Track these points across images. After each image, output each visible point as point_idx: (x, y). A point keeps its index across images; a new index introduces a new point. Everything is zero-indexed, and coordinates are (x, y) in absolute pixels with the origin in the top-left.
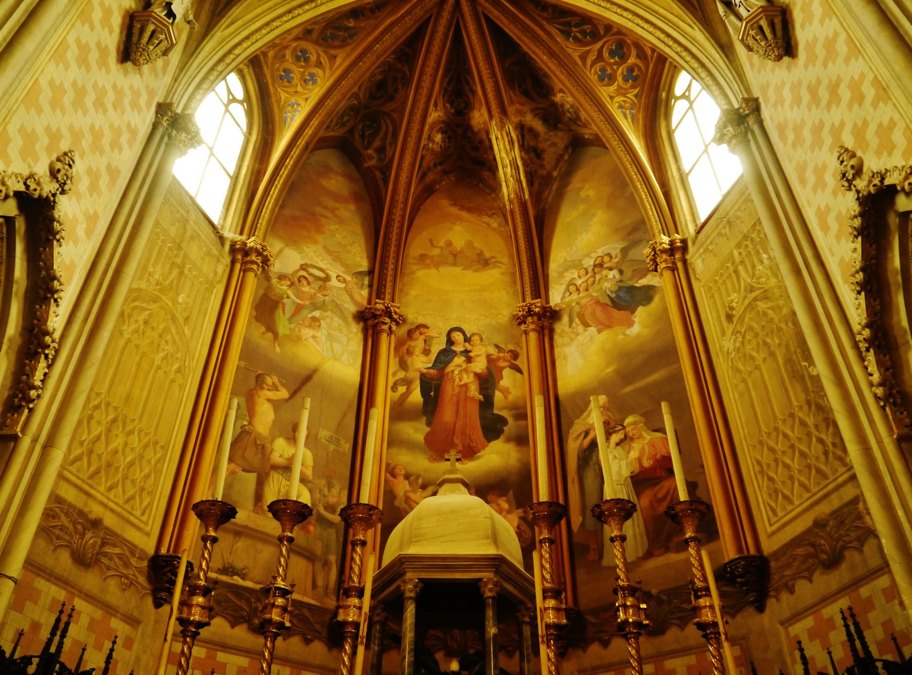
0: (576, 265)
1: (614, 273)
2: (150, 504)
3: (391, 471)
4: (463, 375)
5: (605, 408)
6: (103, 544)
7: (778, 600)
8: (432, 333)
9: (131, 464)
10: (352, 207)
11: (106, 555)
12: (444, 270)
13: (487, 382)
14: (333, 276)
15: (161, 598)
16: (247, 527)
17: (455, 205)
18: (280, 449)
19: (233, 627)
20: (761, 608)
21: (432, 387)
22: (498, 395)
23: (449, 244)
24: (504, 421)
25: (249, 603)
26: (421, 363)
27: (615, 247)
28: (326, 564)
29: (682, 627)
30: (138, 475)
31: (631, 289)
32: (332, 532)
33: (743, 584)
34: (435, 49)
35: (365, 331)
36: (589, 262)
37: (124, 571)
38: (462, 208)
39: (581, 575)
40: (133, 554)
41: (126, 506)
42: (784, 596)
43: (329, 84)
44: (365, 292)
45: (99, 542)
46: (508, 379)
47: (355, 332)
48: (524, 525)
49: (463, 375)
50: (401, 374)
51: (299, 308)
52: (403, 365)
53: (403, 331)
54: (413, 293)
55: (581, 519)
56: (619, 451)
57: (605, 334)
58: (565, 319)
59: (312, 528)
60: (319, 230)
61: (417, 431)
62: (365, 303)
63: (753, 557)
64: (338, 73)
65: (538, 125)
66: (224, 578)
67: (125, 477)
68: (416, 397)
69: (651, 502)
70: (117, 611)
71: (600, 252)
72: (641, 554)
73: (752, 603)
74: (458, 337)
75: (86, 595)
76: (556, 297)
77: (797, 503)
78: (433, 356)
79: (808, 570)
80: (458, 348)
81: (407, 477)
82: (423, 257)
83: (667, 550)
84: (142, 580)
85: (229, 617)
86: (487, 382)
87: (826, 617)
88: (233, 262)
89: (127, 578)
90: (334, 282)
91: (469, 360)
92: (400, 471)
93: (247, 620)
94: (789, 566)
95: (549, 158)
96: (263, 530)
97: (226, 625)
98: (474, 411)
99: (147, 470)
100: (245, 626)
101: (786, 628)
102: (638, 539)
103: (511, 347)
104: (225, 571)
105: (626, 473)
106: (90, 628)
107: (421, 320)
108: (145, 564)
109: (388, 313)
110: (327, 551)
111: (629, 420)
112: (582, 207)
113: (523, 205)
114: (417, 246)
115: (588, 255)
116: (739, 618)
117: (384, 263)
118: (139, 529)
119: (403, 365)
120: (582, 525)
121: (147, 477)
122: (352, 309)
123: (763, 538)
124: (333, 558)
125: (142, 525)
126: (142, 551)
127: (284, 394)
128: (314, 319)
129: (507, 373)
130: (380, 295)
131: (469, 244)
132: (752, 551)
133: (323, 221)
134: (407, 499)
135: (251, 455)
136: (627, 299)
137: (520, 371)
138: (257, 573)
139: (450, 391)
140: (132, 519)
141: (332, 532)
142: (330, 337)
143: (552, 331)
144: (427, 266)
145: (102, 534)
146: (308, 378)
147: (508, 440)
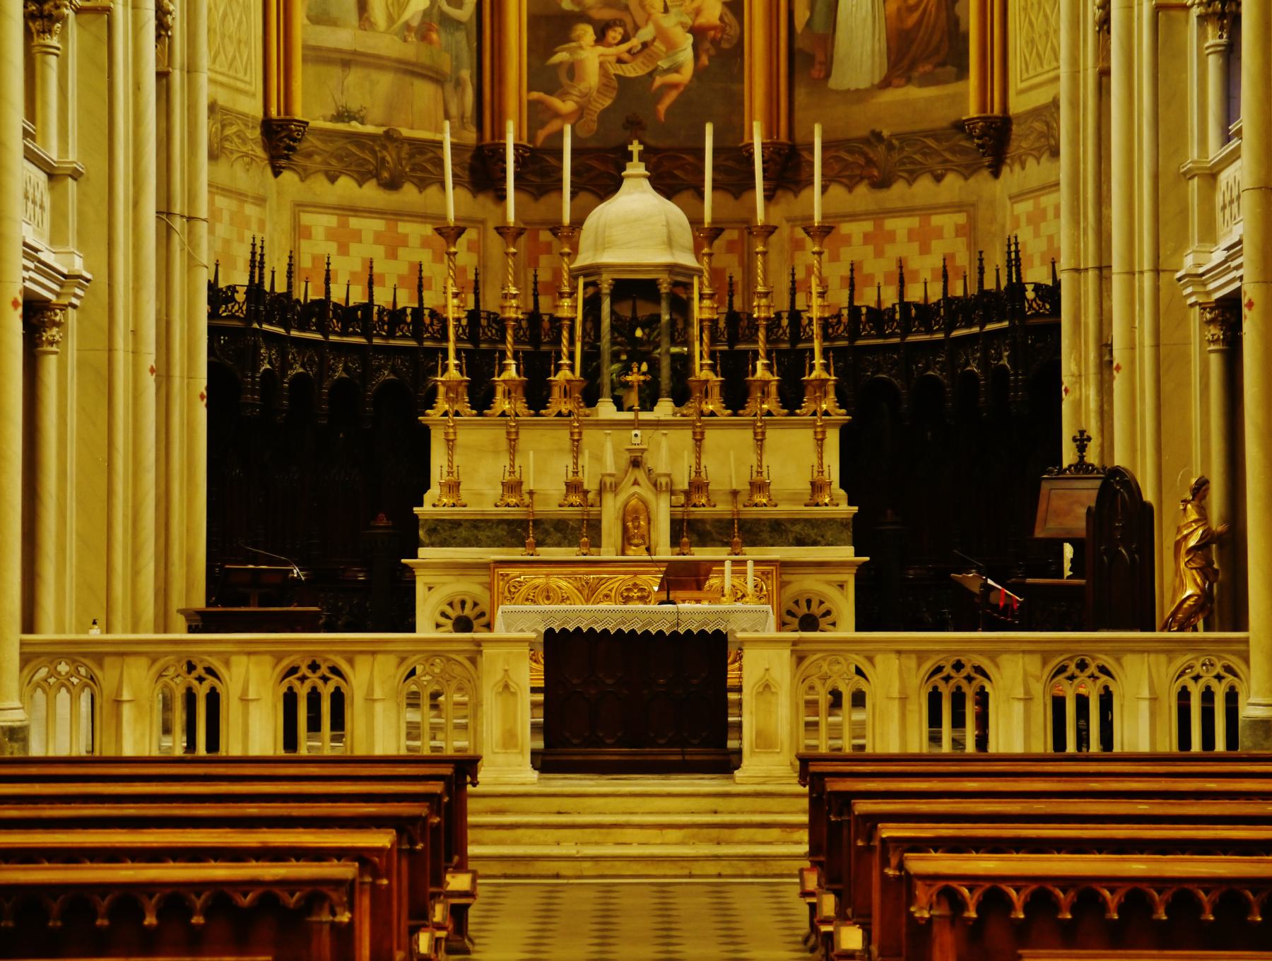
2: (249, 58)
6: (223, 127)
7: (1011, 170)
9: (225, 16)
11: (226, 138)
15: (281, 167)
16: (355, 53)
19: (360, 186)
20: (996, 174)
25: (374, 152)
28: (458, 83)
29: (910, 182)
30: (232, 26)
32: (461, 36)
33: (979, 146)
37: (244, 149)
39: (801, 95)
40: (246, 125)
41: (231, 73)
42: (1017, 168)
45: (219, 126)
48: (729, 14)
55: (808, 14)
59: (434, 36)
63: (996, 117)
66: (341, 126)
67: (223, 36)
69: (899, 10)
70: (246, 196)
72: (877, 81)
73: (989, 167)
75: (223, 189)
77: (1046, 67)
79: (1039, 149)
83: (909, 81)
84: (260, 152)
85: (356, 176)
87: (1042, 206)
89: (247, 155)
93: (376, 175)
94: (1026, 137)
96: (376, 52)
97: (353, 184)
99: (238, 15)
100: (374, 182)
101: (1012, 204)
102: (877, 59)
106: (232, 223)
108: (258, 132)
110: (457, 68)
116: (972, 181)
118: (245, 93)
120: (809, 24)
121: (240, 23)
124: (466, 74)
125: (247, 88)
126: (254, 118)
132: (997, 111)
138: (377, 113)
140: (240, 85)
141: (461, 36)
145: (219, 117)
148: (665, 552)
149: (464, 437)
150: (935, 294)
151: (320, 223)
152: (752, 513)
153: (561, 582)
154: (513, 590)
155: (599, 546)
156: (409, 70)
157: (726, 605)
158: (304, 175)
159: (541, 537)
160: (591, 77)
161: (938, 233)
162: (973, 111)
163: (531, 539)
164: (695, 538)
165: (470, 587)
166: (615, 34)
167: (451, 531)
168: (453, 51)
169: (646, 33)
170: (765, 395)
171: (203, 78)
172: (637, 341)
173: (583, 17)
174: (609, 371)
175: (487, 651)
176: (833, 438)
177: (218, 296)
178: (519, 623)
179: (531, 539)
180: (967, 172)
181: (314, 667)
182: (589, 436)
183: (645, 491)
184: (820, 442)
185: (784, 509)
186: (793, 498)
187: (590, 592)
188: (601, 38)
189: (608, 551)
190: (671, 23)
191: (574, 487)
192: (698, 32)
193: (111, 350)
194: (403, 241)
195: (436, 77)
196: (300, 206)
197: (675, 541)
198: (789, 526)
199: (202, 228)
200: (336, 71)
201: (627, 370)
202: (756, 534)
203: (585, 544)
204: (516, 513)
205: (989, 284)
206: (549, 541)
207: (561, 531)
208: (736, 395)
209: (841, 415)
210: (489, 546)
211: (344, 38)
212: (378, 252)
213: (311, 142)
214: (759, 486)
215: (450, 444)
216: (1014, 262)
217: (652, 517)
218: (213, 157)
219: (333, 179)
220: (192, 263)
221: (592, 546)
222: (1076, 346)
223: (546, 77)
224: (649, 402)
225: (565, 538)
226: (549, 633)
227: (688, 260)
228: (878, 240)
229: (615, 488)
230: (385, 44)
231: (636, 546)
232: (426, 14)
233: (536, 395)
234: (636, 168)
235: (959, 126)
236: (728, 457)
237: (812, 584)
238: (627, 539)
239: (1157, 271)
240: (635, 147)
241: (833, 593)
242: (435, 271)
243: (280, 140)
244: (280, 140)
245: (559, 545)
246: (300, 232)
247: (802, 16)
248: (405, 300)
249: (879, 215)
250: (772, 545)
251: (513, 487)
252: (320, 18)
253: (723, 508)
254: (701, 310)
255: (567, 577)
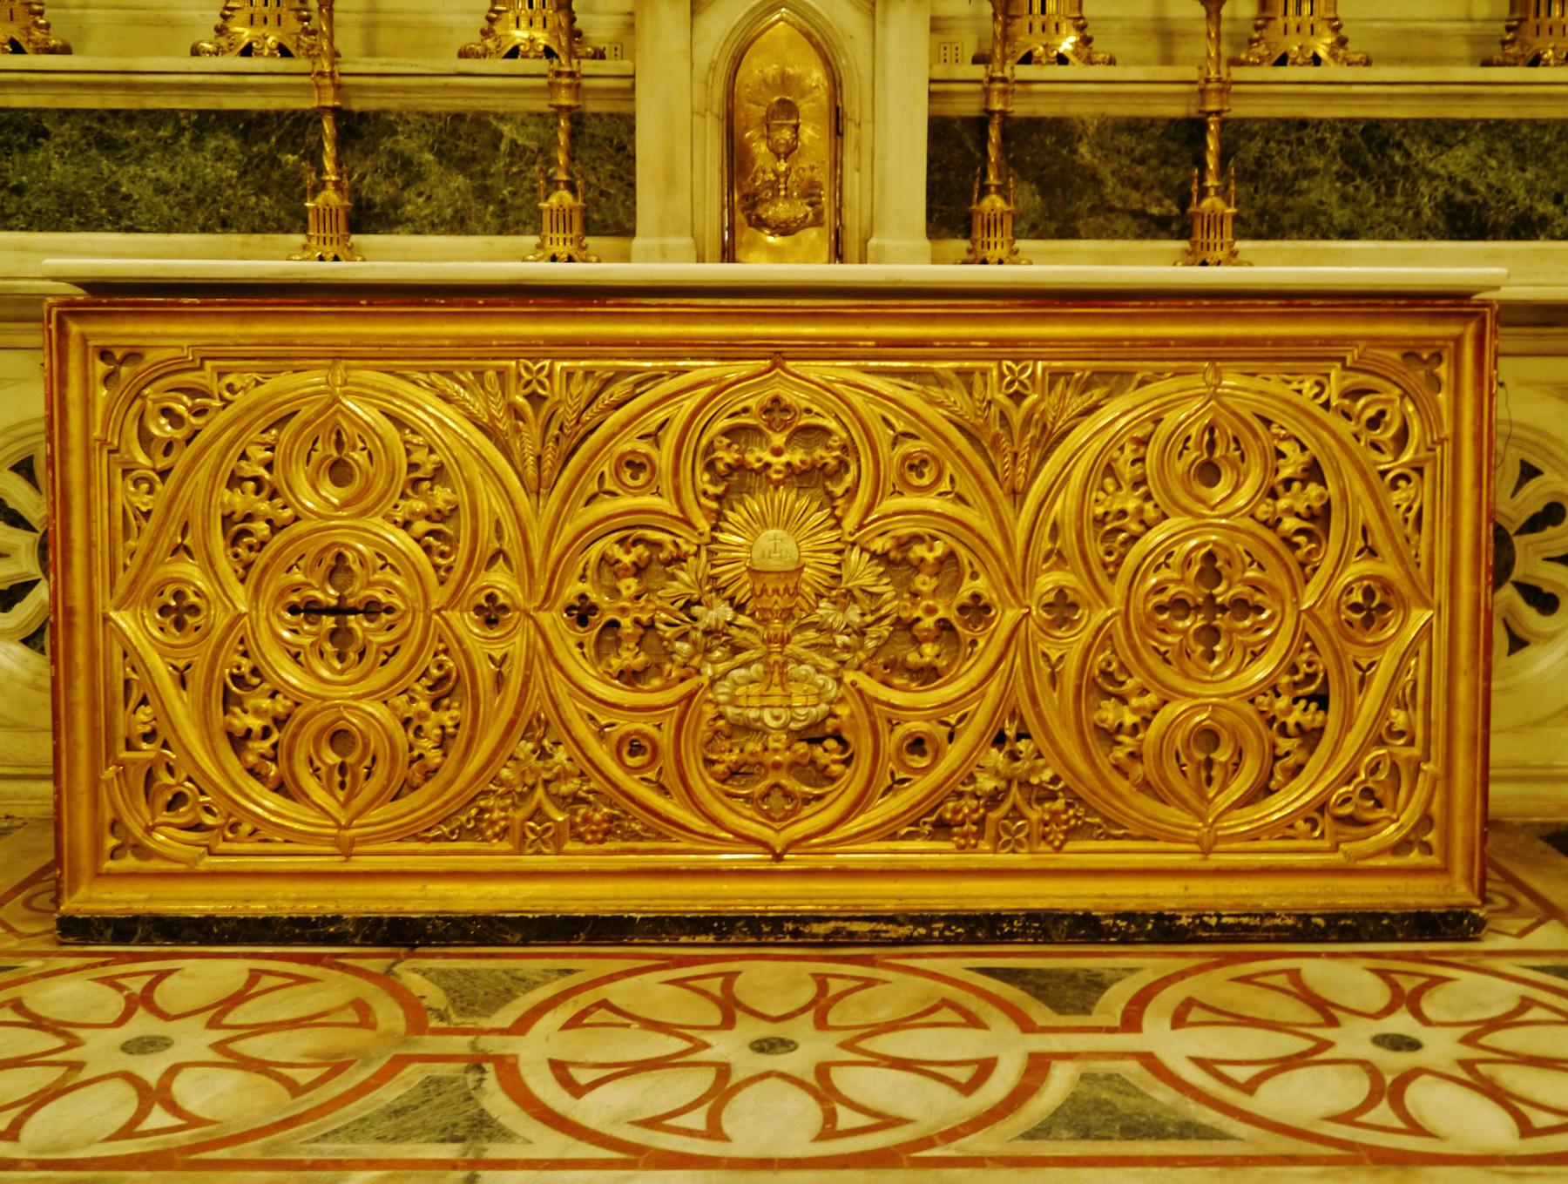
148: (905, 254)
152: (1267, 93)
154: (161, 429)
155: (631, 233)
159: (382, 190)
163: (330, 196)
164: (1029, 198)
179: (330, 196)
185: (1387, 90)
186: (1413, 44)
198: (1421, 152)
202: (1285, 187)
203: (563, 219)
204: (272, 83)
206: (413, 205)
207: (461, 159)
210: (167, 227)
217: (851, 106)
221: (589, 228)
225: (483, 193)
231: (784, 229)
238: (746, 204)
245: (459, 224)
250: (1349, 234)
255: (438, 362)
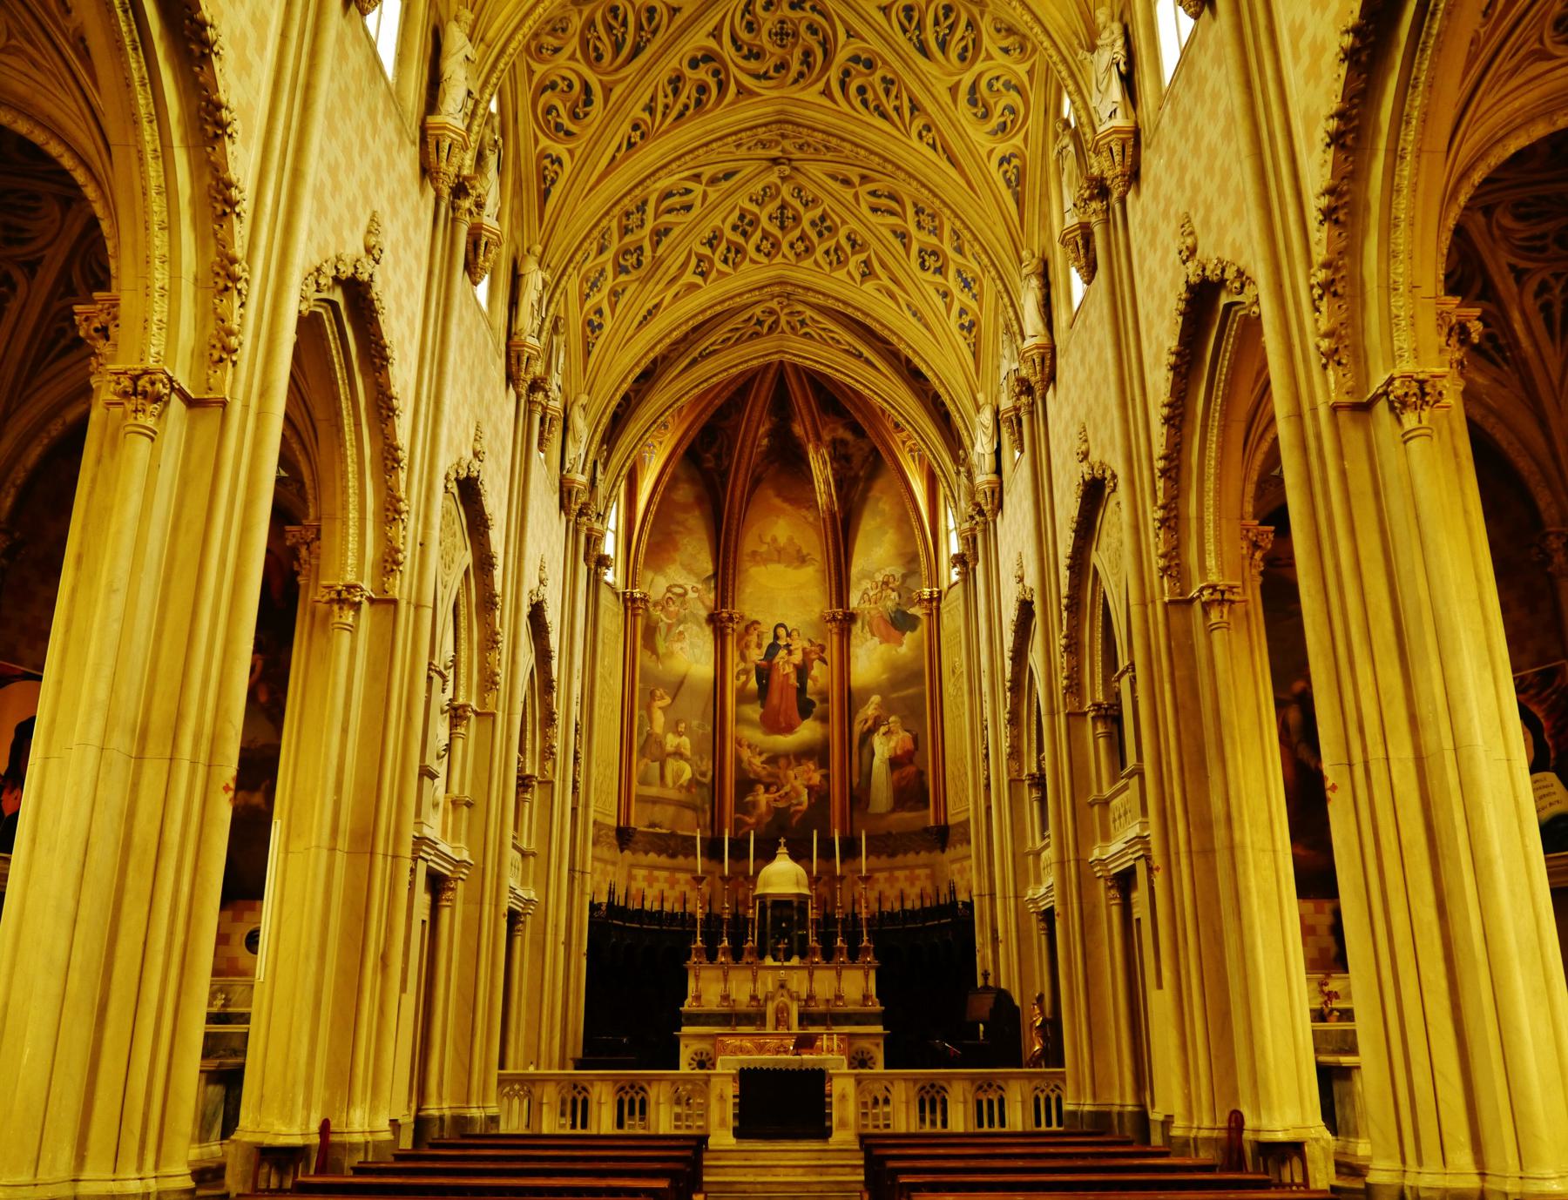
0: (869, 575)
1: (894, 595)
3: (739, 743)
4: (785, 665)
5: (880, 706)
8: (763, 628)
10: (697, 513)
12: (772, 567)
13: (802, 671)
14: (689, 588)
17: (778, 495)
18: (671, 741)
20: (943, 851)
21: (764, 674)
22: (810, 683)
23: (774, 540)
24: (812, 704)
26: (756, 655)
27: (897, 570)
28: (704, 811)
31: (904, 613)
32: (705, 790)
34: (763, 394)
35: (715, 631)
36: (879, 578)
38: (786, 500)
39: (855, 816)
43: (679, 434)
44: (712, 596)
46: (817, 670)
47: (708, 632)
49: (785, 665)
50: (742, 665)
51: (670, 627)
52: (743, 658)
53: (740, 627)
54: (748, 590)
56: (884, 739)
57: (884, 647)
58: (859, 623)
60: (676, 549)
61: (754, 712)
62: (712, 605)
64: (685, 426)
65: (848, 436)
68: (753, 684)
71: (888, 571)
74: (782, 632)
76: (854, 601)
78: (764, 649)
80: (782, 643)
81: (749, 746)
82: (754, 553)
86: (802, 671)
88: (626, 609)
90: (691, 595)
91: (790, 653)
92: (745, 742)
95: (857, 460)
98: (793, 695)
103: (819, 641)
104: (652, 825)
105: (887, 755)
107: (755, 617)
109: (731, 619)
111: (892, 719)
112: (879, 520)
113: (833, 515)
114: (749, 544)
115: (879, 570)
117: (725, 568)
119: (743, 658)
122: (704, 613)
123: (950, 811)
124: (707, 806)
127: (668, 700)
128: (681, 633)
129: (816, 664)
130: (724, 605)
131: (791, 540)
133: (678, 537)
134: (750, 763)
135: (655, 750)
136: (901, 622)
137: (824, 661)
139: (777, 679)
141: (705, 790)
142: (692, 645)
143: (849, 631)
144: (757, 563)
146: (681, 683)
147: (816, 719)
148: (795, 1029)
149: (703, 974)
150: (918, 905)
151: (640, 873)
153: (747, 1044)
156: (681, 805)
157: (825, 1056)
158: (634, 853)
160: (763, 806)
161: (918, 878)
162: (932, 823)
165: (704, 1046)
166: (773, 789)
167: (695, 1019)
168: (701, 797)
169: (787, 788)
170: (842, 955)
171: (591, 810)
172: (782, 930)
173: (759, 781)
174: (770, 942)
175: (713, 1080)
176: (872, 975)
177: (594, 907)
178: (727, 1065)
180: (930, 850)
181: (632, 1087)
182: (761, 973)
183: (786, 999)
184: (867, 976)
185: (851, 1008)
186: (855, 1003)
187: (761, 1049)
188: (767, 791)
189: (769, 1029)
190: (799, 784)
191: (754, 998)
192: (810, 788)
193: (545, 934)
194: (678, 882)
195: (694, 808)
196: (632, 866)
197: (800, 1023)
199: (588, 877)
200: (650, 806)
201: (778, 943)
204: (725, 1010)
205: (942, 901)
208: (829, 954)
209: (876, 963)
211: (654, 791)
212: (666, 886)
213: (637, 837)
214: (839, 997)
215: (697, 977)
216: (953, 891)
218: (594, 844)
219: (646, 853)
220: (582, 893)
222: (982, 931)
223: (743, 807)
224: (788, 959)
226: (742, 1070)
227: (806, 891)
228: (891, 880)
229: (773, 998)
230: (672, 794)
232: (690, 780)
233: (736, 954)
234: (783, 850)
235: (926, 830)
236: (824, 984)
237: (865, 1044)
238: (778, 1022)
239: (1016, 897)
240: (782, 840)
241: (873, 1048)
242: (692, 895)
243: (624, 837)
244: (624, 837)
246: (631, 877)
247: (856, 780)
248: (678, 909)
249: (892, 869)
251: (726, 997)
252: (644, 782)
253: (822, 1008)
254: (812, 914)
